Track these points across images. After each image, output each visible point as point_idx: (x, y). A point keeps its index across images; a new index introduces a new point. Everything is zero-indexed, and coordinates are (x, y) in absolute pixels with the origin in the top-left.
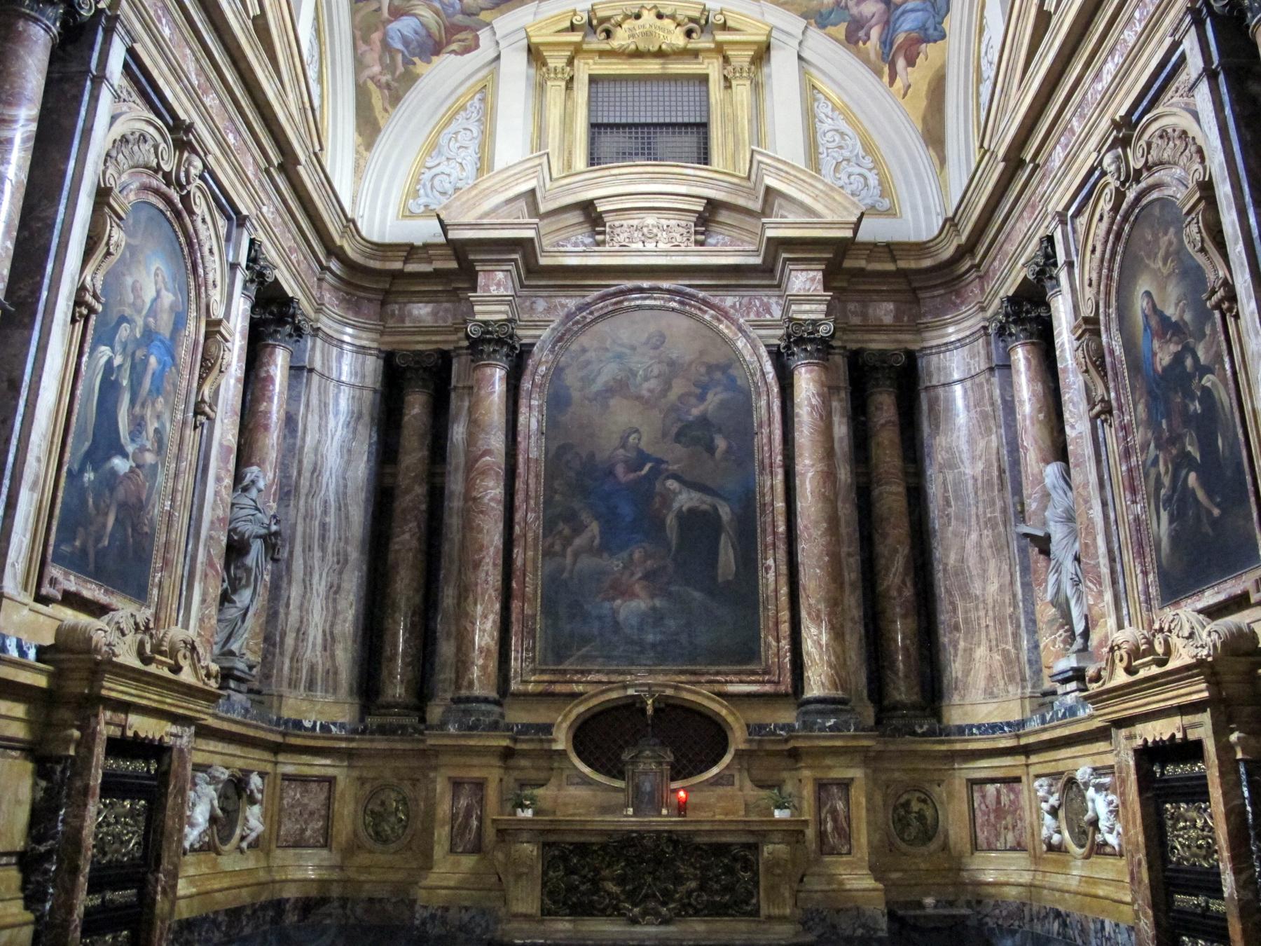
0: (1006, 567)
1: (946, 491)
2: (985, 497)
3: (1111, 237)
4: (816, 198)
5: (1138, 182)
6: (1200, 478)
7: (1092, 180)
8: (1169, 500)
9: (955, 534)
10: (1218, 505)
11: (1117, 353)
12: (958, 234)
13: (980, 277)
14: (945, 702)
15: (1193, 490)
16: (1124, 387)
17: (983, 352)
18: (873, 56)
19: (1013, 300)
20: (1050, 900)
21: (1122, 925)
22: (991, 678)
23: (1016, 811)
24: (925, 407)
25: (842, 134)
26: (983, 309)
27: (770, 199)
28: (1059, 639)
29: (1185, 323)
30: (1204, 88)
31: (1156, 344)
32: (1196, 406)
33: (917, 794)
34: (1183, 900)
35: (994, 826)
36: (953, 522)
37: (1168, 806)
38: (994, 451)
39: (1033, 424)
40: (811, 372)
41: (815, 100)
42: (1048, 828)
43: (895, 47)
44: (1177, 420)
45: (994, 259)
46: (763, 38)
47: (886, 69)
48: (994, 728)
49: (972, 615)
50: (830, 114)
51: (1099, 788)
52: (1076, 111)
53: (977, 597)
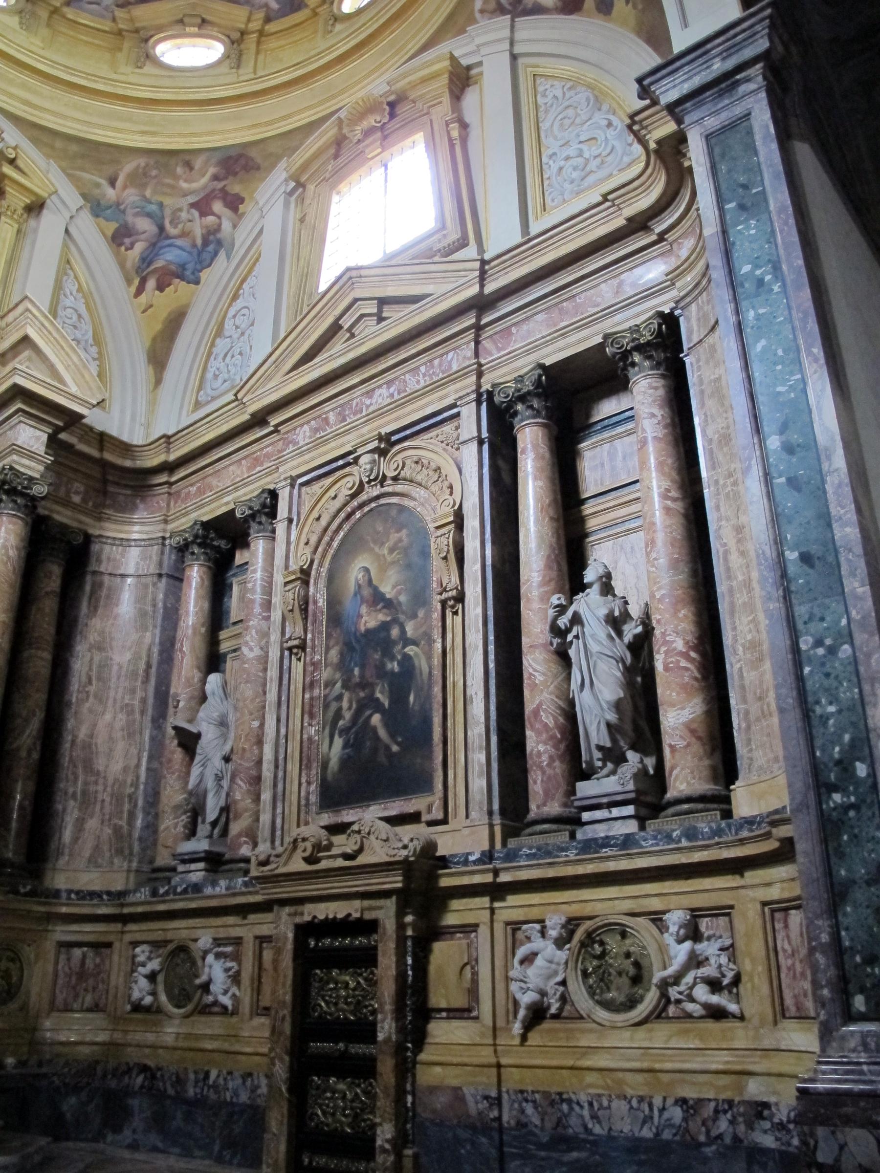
0: (134, 751)
1: (90, 669)
2: (127, 684)
3: (342, 515)
4: (67, 368)
5: (382, 486)
7: (334, 465)
8: (344, 732)
9: (91, 711)
10: (398, 744)
11: (320, 604)
12: (168, 451)
13: (169, 494)
14: (50, 865)
16: (321, 633)
17: (155, 558)
18: (129, 265)
19: (206, 525)
20: (133, 1056)
21: (236, 1074)
22: (97, 848)
23: (99, 973)
24: (88, 588)
25: (80, 316)
26: (166, 522)
27: (21, 347)
28: (181, 824)
29: (400, 603)
30: (474, 446)
31: (364, 609)
32: (395, 666)
33: (9, 953)
34: (316, 1046)
35: (74, 988)
36: (91, 699)
37: (318, 971)
38: (145, 647)
39: (194, 633)
40: (15, 524)
41: (66, 274)
42: (140, 991)
43: (152, 268)
44: (370, 673)
45: (192, 485)
46: (45, 195)
47: (137, 282)
48: (92, 895)
49: (92, 788)
50: (74, 293)
51: (218, 956)
52: (336, 408)
53: (98, 773)
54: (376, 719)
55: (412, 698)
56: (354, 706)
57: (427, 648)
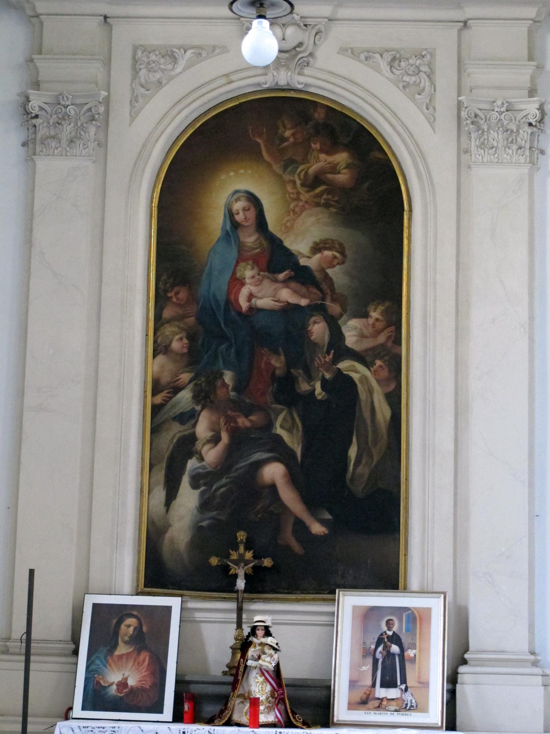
6: (293, 478)
10: (323, 522)
15: (273, 487)
54: (274, 472)
55: (353, 452)
56: (225, 438)
57: (385, 373)
